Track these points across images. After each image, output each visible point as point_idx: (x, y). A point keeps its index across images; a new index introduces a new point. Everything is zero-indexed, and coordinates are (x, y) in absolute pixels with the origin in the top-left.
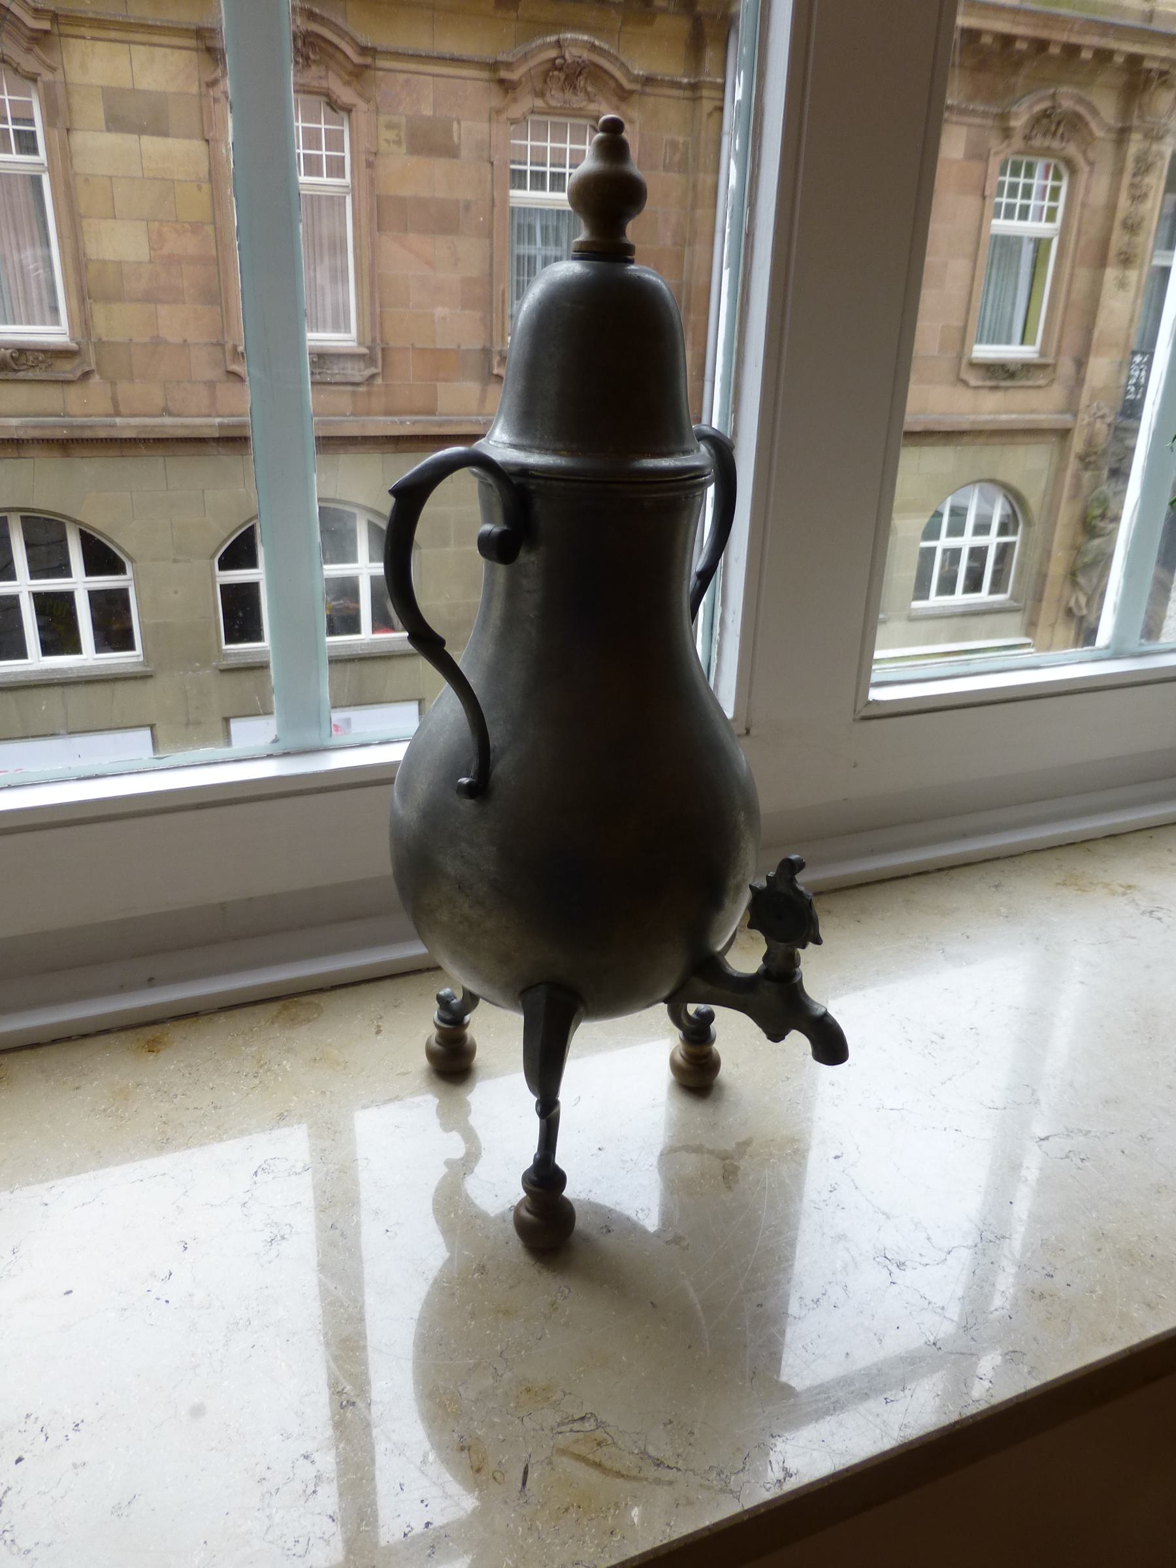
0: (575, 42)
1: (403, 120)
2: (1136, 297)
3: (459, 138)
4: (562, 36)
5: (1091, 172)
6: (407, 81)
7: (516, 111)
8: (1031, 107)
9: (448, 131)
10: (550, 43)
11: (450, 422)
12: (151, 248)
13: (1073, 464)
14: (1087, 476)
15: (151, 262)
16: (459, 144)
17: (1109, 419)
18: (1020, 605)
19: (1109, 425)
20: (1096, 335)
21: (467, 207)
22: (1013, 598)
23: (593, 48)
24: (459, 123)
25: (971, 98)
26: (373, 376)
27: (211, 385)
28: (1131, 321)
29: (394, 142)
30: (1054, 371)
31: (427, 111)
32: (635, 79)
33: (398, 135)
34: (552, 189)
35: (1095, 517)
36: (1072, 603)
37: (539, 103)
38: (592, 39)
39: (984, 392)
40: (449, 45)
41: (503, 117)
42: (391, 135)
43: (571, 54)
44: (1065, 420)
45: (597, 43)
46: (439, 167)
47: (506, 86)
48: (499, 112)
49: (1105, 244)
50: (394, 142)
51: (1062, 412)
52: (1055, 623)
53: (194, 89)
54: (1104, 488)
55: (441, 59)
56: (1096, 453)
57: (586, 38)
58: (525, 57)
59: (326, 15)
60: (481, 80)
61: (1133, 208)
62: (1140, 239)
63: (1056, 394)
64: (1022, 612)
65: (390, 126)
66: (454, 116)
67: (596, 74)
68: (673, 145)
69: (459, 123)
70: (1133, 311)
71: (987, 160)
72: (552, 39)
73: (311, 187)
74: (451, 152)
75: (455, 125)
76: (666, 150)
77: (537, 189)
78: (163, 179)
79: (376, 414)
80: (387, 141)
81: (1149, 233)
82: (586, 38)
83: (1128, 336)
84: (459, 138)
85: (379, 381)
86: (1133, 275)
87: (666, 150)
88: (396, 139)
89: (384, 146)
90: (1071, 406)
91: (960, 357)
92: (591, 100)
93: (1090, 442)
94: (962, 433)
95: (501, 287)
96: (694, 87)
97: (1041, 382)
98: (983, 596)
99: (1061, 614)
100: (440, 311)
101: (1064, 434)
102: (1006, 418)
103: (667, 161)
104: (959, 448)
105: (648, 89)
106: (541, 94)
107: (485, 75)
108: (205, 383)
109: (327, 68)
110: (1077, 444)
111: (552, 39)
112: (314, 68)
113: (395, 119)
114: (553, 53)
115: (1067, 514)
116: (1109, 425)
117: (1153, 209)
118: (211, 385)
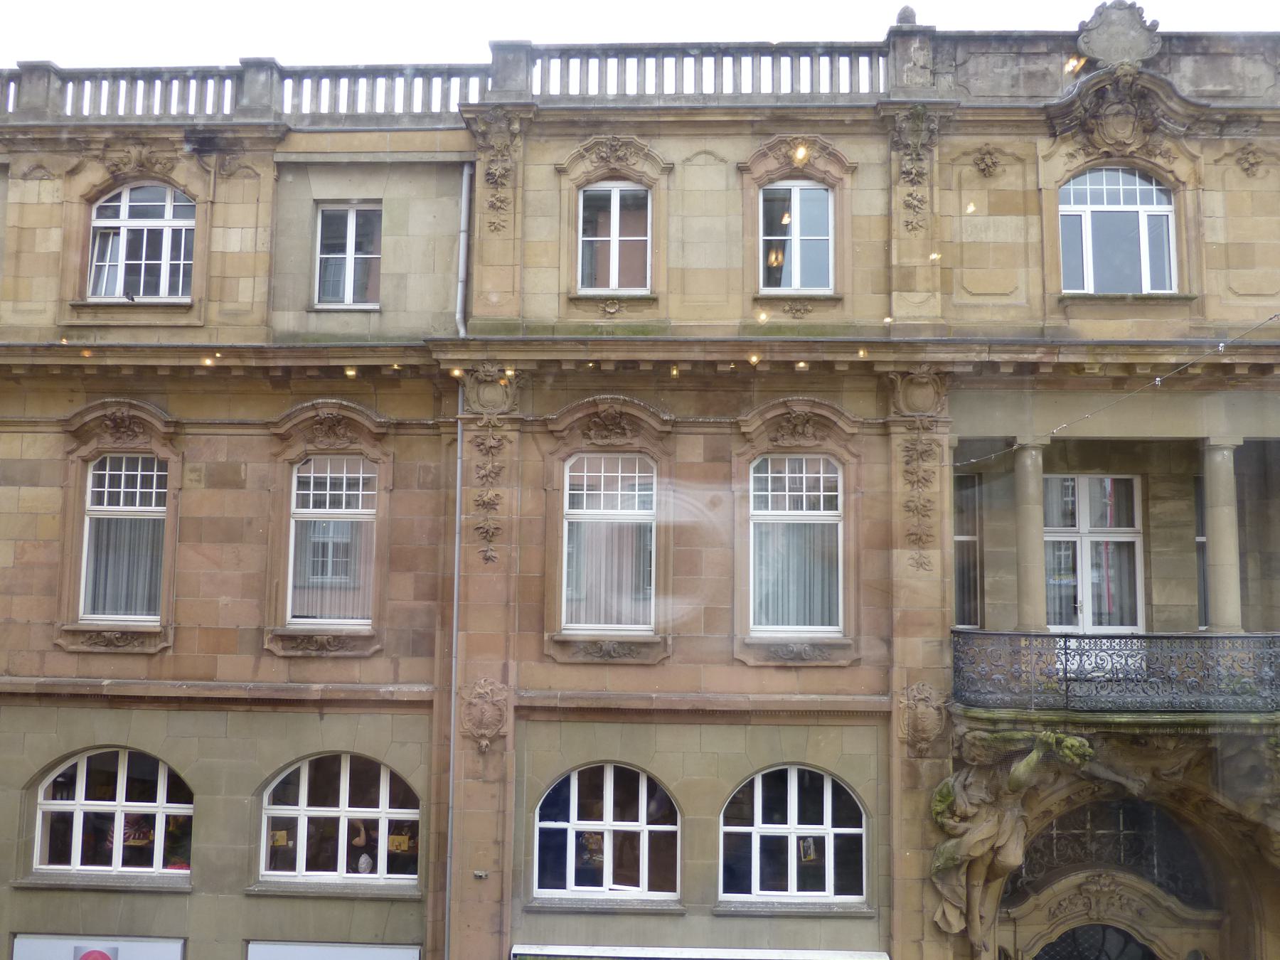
0: (326, 405)
1: (204, 466)
2: (944, 575)
3: (246, 475)
4: (314, 402)
5: (859, 464)
6: (209, 440)
7: (292, 453)
8: (761, 414)
9: (237, 472)
10: (307, 407)
11: (227, 688)
12: (15, 558)
13: (899, 754)
14: (925, 765)
15: (13, 567)
16: (245, 480)
17: (940, 703)
18: (872, 911)
19: (938, 709)
20: (897, 614)
21: (250, 523)
22: (868, 903)
23: (341, 407)
24: (246, 465)
25: (704, 412)
26: (165, 649)
27: (42, 653)
28: (943, 599)
29: (196, 481)
30: (857, 649)
31: (222, 458)
32: (380, 425)
33: (199, 476)
34: (772, 509)
35: (938, 813)
36: (938, 917)
37: (310, 447)
38: (339, 401)
39: (766, 672)
40: (240, 414)
41: (280, 459)
42: (194, 476)
43: (323, 413)
44: (876, 702)
45: (345, 403)
46: (229, 495)
47: (283, 438)
48: (276, 455)
49: (888, 526)
50: (196, 481)
51: (878, 694)
52: (923, 939)
53: (59, 456)
54: (950, 780)
55: (231, 424)
56: (926, 740)
57: (334, 401)
58: (288, 417)
59: (141, 404)
60: (59, 433)
61: (915, 493)
62: (934, 519)
63: (867, 676)
64: (876, 919)
65: (193, 470)
66: (242, 460)
67: (350, 424)
68: (427, 469)
69: (246, 465)
70: (944, 591)
71: (731, 462)
72: (309, 404)
73: (352, 516)
74: (239, 485)
75: (243, 466)
76: (419, 474)
77: (760, 509)
78: (31, 513)
79: (166, 679)
80: (191, 480)
81: (942, 513)
82: (334, 401)
83: (944, 615)
84: (246, 475)
85: (170, 653)
86: (934, 555)
87: (419, 474)
88: (197, 478)
89: (187, 483)
90: (887, 690)
91: (732, 638)
92: (351, 442)
93: (916, 729)
94: (713, 713)
95: (276, 581)
96: (436, 426)
97: (843, 662)
98: (828, 896)
99: (927, 928)
100: (224, 600)
101: (887, 716)
102: (813, 699)
103: (421, 480)
104: (749, 728)
105: (402, 431)
106: (310, 441)
107: (59, 429)
108: (38, 652)
109: (151, 437)
110: (900, 729)
111: (309, 404)
112: (141, 437)
113: (198, 465)
114: (312, 414)
115: (903, 808)
116: (938, 709)
117: (941, 492)
118: (42, 653)
